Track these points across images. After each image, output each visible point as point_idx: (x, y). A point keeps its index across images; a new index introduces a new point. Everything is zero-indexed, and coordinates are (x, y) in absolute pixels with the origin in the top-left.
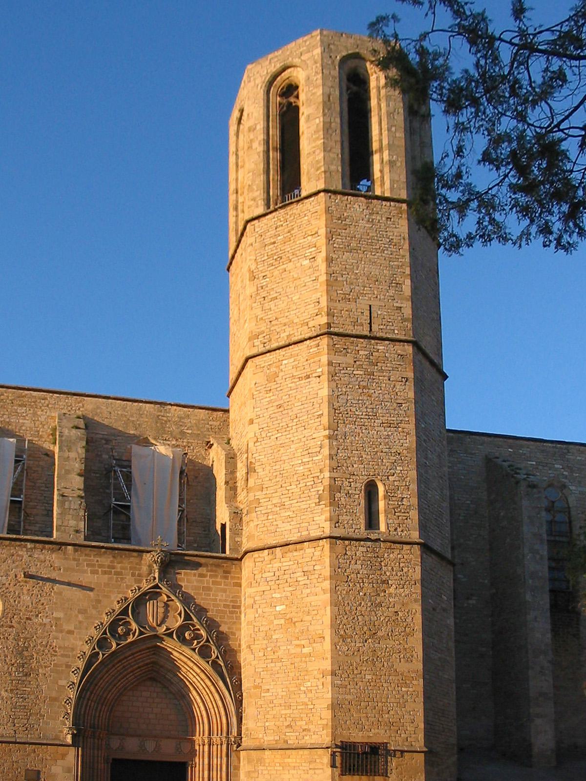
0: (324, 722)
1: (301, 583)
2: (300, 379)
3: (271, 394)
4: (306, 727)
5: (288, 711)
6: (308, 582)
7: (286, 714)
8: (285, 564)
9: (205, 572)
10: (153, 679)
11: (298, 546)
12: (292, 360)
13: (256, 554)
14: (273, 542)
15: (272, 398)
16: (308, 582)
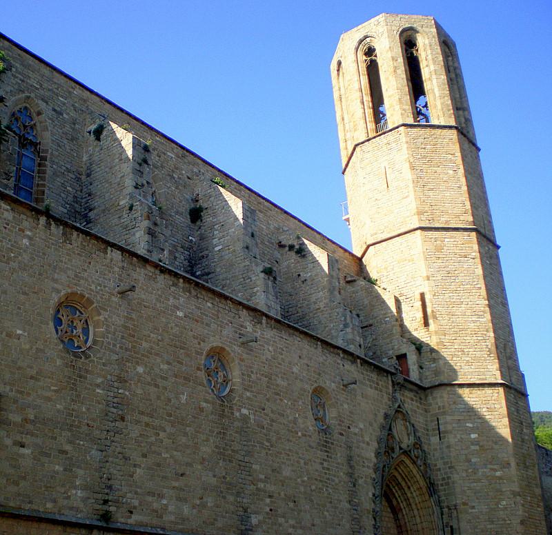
3: (440, 261)
5: (492, 526)
7: (491, 529)
8: (472, 399)
9: (413, 397)
12: (452, 240)
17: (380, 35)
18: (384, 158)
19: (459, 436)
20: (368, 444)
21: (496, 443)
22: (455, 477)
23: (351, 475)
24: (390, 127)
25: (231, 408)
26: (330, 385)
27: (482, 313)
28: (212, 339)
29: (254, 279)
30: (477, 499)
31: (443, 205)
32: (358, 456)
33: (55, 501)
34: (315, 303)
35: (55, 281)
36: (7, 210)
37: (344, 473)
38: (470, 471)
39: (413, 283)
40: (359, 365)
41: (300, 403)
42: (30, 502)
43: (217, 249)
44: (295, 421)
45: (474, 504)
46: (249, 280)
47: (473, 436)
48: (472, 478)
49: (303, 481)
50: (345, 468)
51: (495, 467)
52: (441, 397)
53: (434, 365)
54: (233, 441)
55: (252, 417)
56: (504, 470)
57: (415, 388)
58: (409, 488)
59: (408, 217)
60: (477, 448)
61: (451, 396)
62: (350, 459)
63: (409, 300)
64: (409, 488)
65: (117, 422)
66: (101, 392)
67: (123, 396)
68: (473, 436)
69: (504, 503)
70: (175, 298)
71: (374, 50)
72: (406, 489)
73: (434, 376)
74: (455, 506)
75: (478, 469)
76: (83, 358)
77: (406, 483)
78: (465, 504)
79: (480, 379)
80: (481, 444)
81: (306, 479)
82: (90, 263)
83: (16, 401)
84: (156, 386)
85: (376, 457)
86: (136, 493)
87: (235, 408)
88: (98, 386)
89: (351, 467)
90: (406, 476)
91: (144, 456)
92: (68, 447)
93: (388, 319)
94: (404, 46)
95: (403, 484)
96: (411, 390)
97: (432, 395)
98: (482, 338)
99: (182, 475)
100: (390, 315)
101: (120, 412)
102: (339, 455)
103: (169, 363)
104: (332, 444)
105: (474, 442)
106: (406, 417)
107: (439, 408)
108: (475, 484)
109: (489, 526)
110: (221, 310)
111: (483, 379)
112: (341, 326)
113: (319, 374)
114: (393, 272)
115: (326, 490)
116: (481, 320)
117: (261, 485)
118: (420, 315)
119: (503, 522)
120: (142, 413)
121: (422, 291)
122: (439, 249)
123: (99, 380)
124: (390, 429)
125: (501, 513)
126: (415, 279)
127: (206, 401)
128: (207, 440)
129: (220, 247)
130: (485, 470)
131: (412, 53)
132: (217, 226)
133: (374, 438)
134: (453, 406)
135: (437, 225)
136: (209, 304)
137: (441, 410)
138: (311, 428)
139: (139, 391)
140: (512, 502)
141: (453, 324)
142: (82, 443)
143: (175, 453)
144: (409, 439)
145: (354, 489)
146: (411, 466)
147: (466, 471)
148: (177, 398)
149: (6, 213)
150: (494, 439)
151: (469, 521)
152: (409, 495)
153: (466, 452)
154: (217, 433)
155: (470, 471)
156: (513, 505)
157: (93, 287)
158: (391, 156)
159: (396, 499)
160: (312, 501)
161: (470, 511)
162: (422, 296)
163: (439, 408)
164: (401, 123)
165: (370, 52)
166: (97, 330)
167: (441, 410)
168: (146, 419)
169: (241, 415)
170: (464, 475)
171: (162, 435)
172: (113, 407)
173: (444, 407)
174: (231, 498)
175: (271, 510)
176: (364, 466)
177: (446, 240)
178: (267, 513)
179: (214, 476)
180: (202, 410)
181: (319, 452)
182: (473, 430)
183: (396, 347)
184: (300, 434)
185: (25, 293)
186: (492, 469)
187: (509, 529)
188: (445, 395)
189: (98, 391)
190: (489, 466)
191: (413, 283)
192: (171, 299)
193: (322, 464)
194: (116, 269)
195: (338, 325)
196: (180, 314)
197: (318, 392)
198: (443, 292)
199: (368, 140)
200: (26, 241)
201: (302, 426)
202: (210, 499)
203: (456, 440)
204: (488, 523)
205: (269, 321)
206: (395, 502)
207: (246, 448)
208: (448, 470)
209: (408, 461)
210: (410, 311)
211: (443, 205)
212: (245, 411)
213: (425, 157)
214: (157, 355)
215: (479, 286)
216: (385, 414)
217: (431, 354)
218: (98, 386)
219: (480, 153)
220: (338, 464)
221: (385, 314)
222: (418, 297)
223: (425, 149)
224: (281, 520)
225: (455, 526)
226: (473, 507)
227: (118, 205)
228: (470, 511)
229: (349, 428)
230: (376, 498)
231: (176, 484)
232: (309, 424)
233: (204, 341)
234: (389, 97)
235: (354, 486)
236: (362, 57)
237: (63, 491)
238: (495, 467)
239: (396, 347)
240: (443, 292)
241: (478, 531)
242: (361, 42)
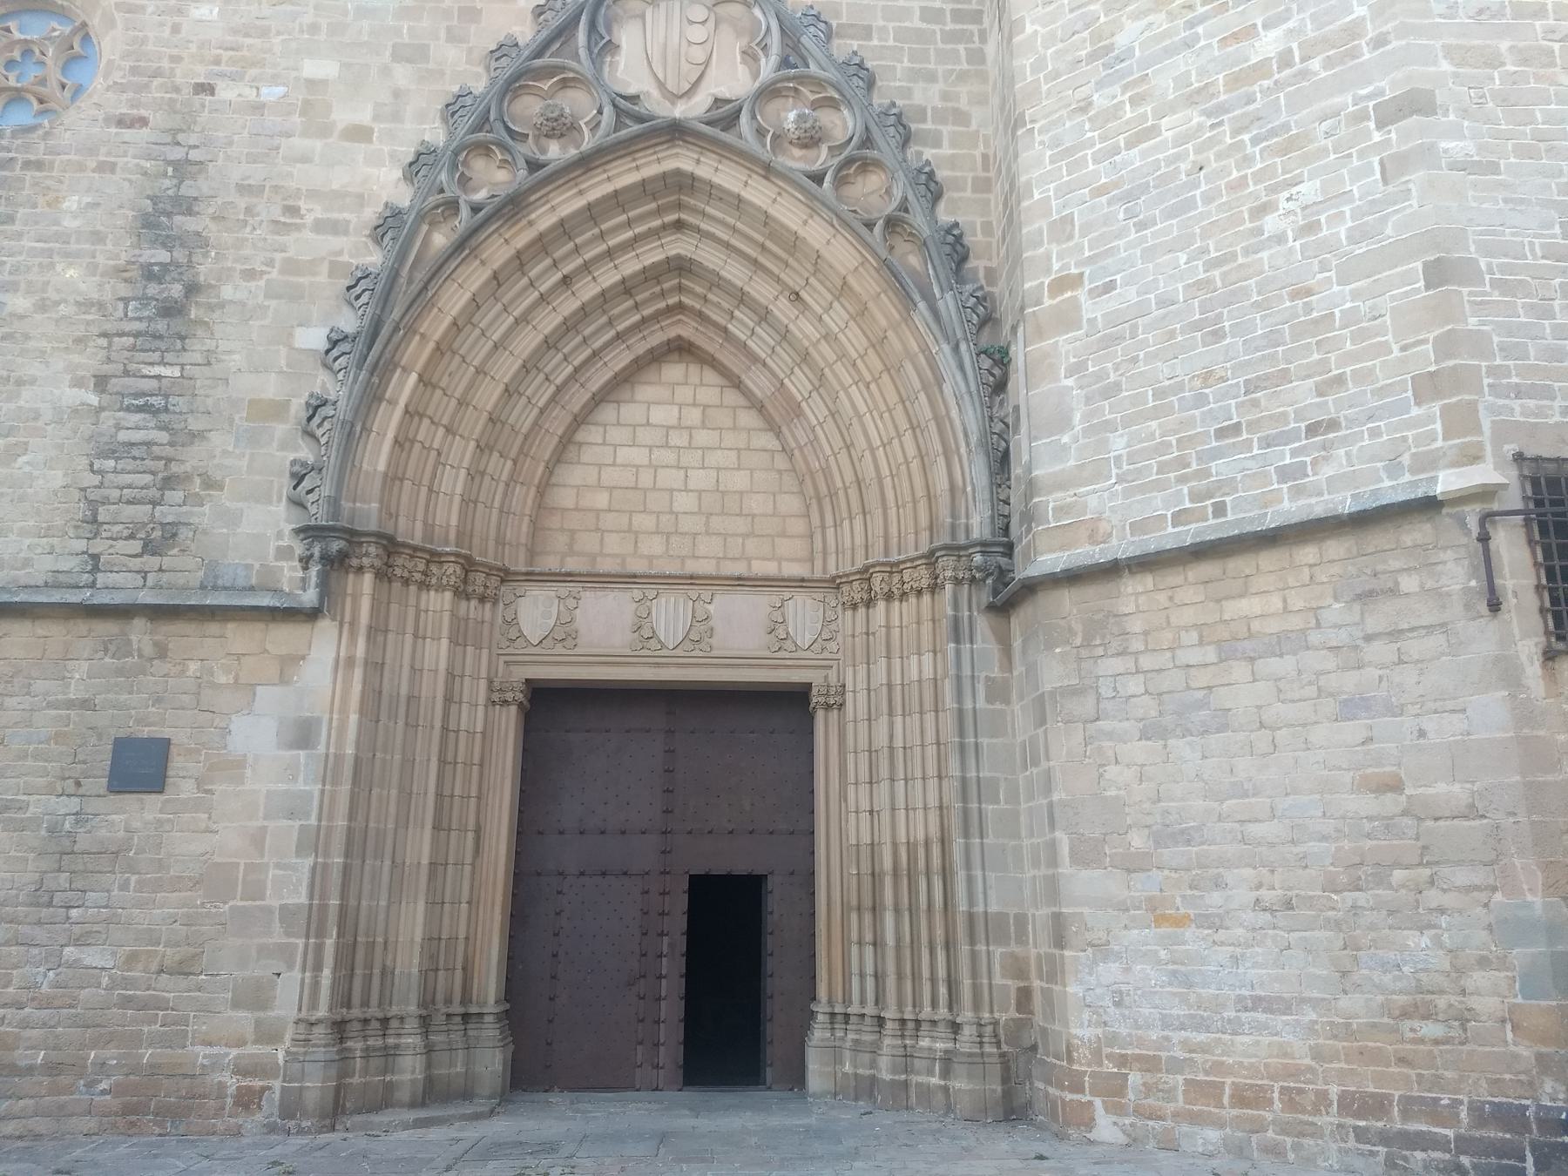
10: (681, 349)
20: (359, 134)
32: (243, 189)
37: (92, 269)
50: (120, 249)
58: (796, 297)
64: (796, 297)
72: (783, 310)
77: (778, 280)
95: (762, 290)
144: (755, 75)
145: (161, 326)
146: (758, 193)
152: (805, 329)
159: (764, 364)
176: (278, 227)
206: (758, 382)
209: (728, 177)
220: (63, 238)
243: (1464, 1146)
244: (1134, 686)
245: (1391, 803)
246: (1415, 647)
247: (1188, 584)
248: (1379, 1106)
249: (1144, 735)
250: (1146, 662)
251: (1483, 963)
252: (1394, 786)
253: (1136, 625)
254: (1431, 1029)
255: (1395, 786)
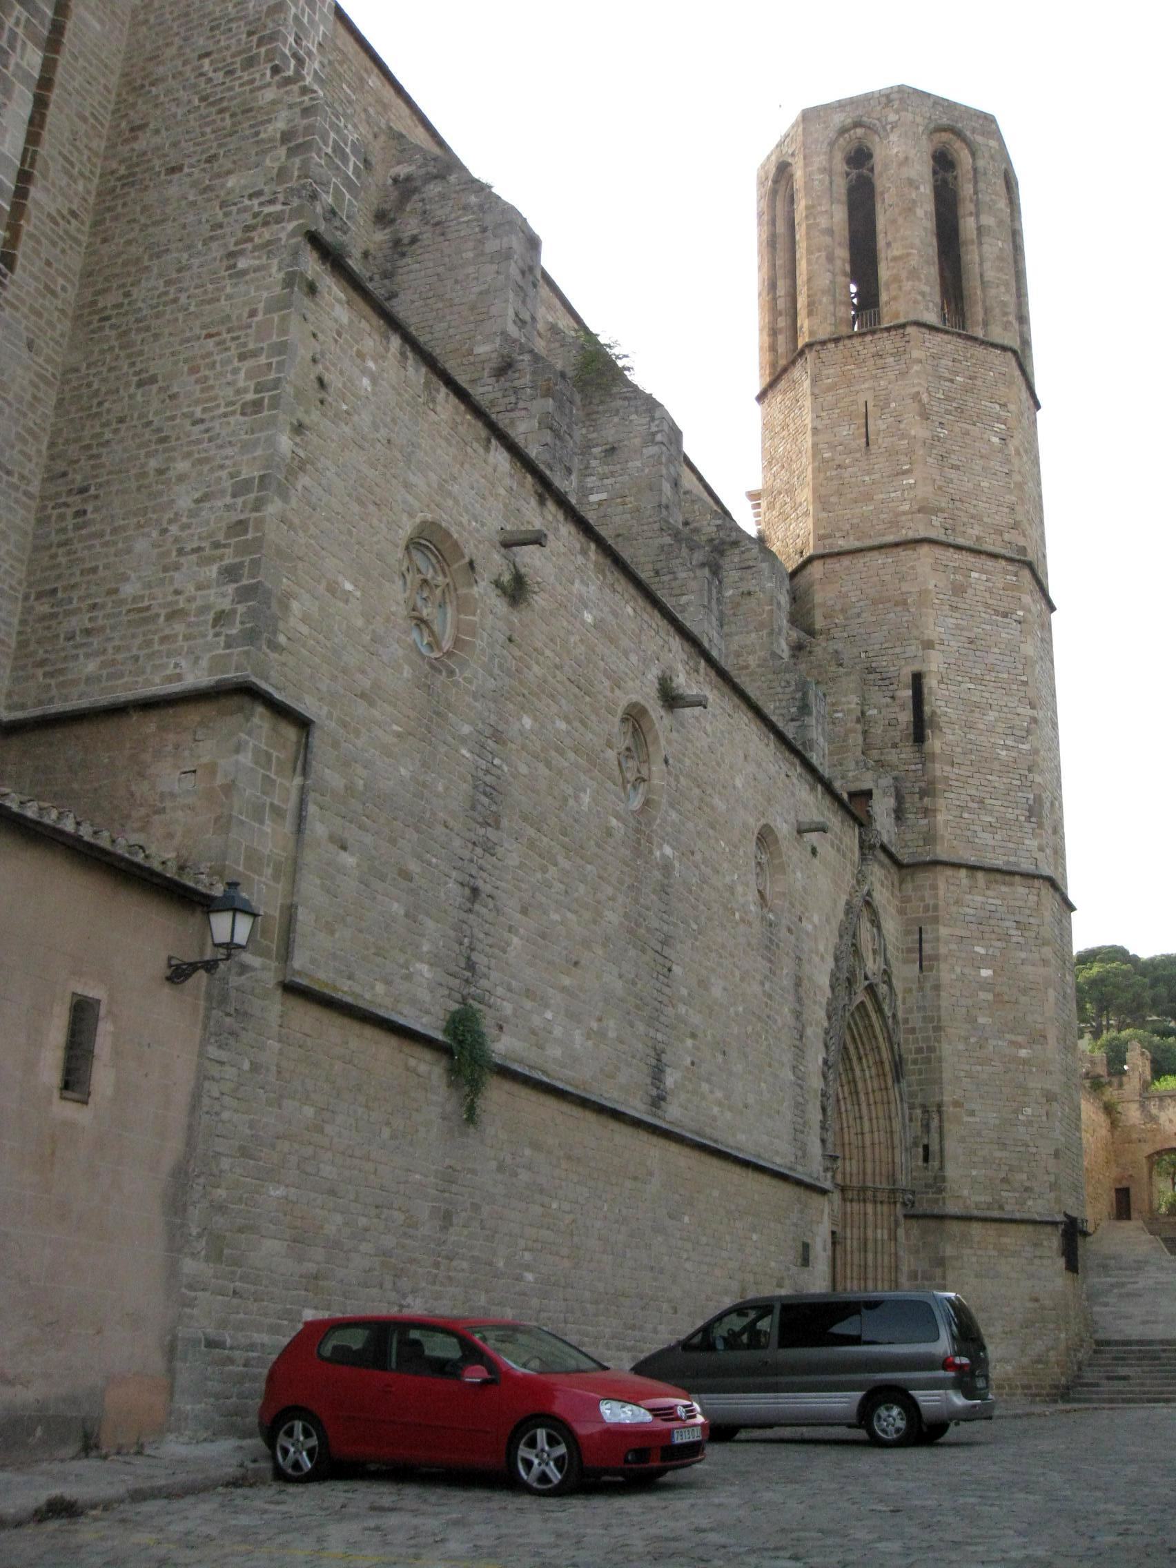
0: (1052, 1179)
1: (1014, 939)
2: (997, 613)
3: (958, 615)
4: (1027, 1184)
5: (1005, 1154)
6: (1021, 940)
8: (991, 901)
11: (1007, 878)
12: (984, 577)
13: (949, 872)
14: (972, 860)
15: (960, 622)
16: (1021, 940)
17: (889, 127)
18: (866, 385)
19: (958, 970)
21: (1024, 991)
22: (946, 1049)
23: (798, 1015)
24: (885, 325)
25: (650, 841)
26: (783, 829)
27: (1024, 734)
28: (631, 683)
29: (682, 575)
30: (981, 1097)
31: (974, 502)
33: (388, 983)
34: (738, 655)
35: (407, 486)
36: (339, 301)
38: (973, 1040)
39: (897, 650)
40: (820, 796)
41: (741, 853)
42: (350, 977)
43: (594, 498)
44: (731, 889)
45: (973, 1107)
46: (670, 577)
47: (986, 973)
48: (975, 1054)
49: (737, 1014)
51: (1020, 1039)
52: (934, 887)
53: (925, 821)
54: (648, 909)
55: (677, 864)
56: (1034, 1046)
57: (886, 861)
58: (860, 1059)
59: (904, 513)
60: (990, 997)
61: (952, 888)
62: (798, 983)
63: (887, 682)
64: (860, 1059)
65: (489, 829)
66: (468, 755)
67: (499, 772)
68: (986, 973)
69: (1029, 1111)
70: (582, 581)
71: (870, 156)
73: (921, 843)
74: (939, 1106)
75: (987, 1039)
76: (444, 673)
77: (857, 1048)
78: (957, 1104)
79: (1008, 862)
80: (998, 989)
81: (741, 1009)
82: (462, 465)
83: (336, 745)
84: (548, 765)
85: (832, 988)
86: (510, 990)
87: (656, 840)
88: (463, 740)
89: (799, 1000)
90: (860, 1035)
91: (524, 911)
92: (414, 867)
93: (840, 715)
94: (931, 162)
96: (882, 865)
97: (913, 881)
98: (1018, 783)
99: (576, 964)
100: (845, 707)
101: (494, 808)
102: (785, 971)
103: (569, 722)
104: (777, 945)
105: (985, 985)
106: (876, 922)
107: (926, 908)
108: (979, 1068)
109: (998, 1154)
110: (645, 626)
111: (1015, 864)
112: (793, 710)
113: (769, 800)
114: (860, 620)
115: (766, 1039)
116: (1021, 746)
117: (682, 1009)
118: (906, 717)
119: (1022, 1149)
120: (525, 819)
121: (916, 667)
122: (959, 590)
123: (466, 729)
124: (854, 936)
125: (1022, 1129)
126: (905, 643)
127: (618, 816)
128: (613, 899)
129: (603, 496)
130: (1000, 1043)
131: (945, 182)
132: (599, 449)
133: (831, 950)
134: (954, 909)
135: (961, 541)
136: (629, 610)
137: (930, 913)
138: (752, 908)
139: (523, 769)
140: (1043, 1112)
141: (969, 746)
142: (434, 860)
143: (569, 915)
146: (873, 1016)
147: (967, 1038)
148: (577, 798)
149: (338, 307)
150: (1022, 984)
151: (962, 1140)
152: (858, 1073)
153: (970, 1002)
154: (629, 887)
155: (973, 1040)
156: (1044, 1118)
157: (465, 520)
158: (882, 383)
160: (746, 1056)
161: (966, 1119)
162: (917, 680)
163: (926, 908)
164: (912, 318)
165: (860, 158)
166: (462, 616)
167: (930, 913)
168: (531, 832)
169: (663, 855)
170: (961, 1047)
171: (553, 870)
172: (485, 794)
173: (936, 908)
174: (641, 1027)
175: (693, 1063)
177: (974, 575)
178: (687, 1069)
179: (621, 976)
180: (609, 832)
181: (759, 958)
182: (985, 961)
183: (850, 774)
184: (737, 916)
185: (361, 502)
186: (1012, 1043)
187: (1034, 1164)
188: (942, 885)
189: (464, 752)
190: (1008, 1036)
191: (897, 650)
192: (577, 582)
193: (762, 984)
194: (502, 491)
195: (788, 707)
196: (588, 618)
197: (765, 837)
198: (960, 679)
199: (836, 340)
200: (366, 382)
201: (742, 900)
202: (612, 1023)
203: (954, 977)
204: (996, 1147)
205: (709, 669)
207: (665, 927)
208: (931, 1033)
210: (887, 706)
211: (974, 502)
212: (668, 850)
213: (948, 399)
214: (552, 696)
215: (1024, 678)
216: (848, 903)
217: (921, 799)
218: (463, 740)
219: (1039, 414)
221: (833, 705)
222: (908, 680)
223: (952, 381)
224: (705, 1087)
225: (934, 1147)
226: (972, 1113)
227: (470, 352)
228: (966, 1119)
229: (800, 919)
230: (829, 1068)
231: (567, 981)
232: (750, 899)
233: (619, 687)
234: (895, 259)
235: (801, 1037)
236: (840, 166)
237: (402, 961)
238: (1020, 1039)
239: (850, 774)
240: (960, 679)
241: (976, 1159)
242: (843, 131)
243: (1048, 1395)
244: (974, 1259)
245: (1036, 1305)
246: (1045, 1262)
247: (992, 1229)
248: (1028, 1387)
249: (976, 1276)
250: (979, 1252)
251: (1052, 1348)
252: (1037, 1300)
253: (976, 1239)
254: (1040, 1366)
255: (1037, 1300)
